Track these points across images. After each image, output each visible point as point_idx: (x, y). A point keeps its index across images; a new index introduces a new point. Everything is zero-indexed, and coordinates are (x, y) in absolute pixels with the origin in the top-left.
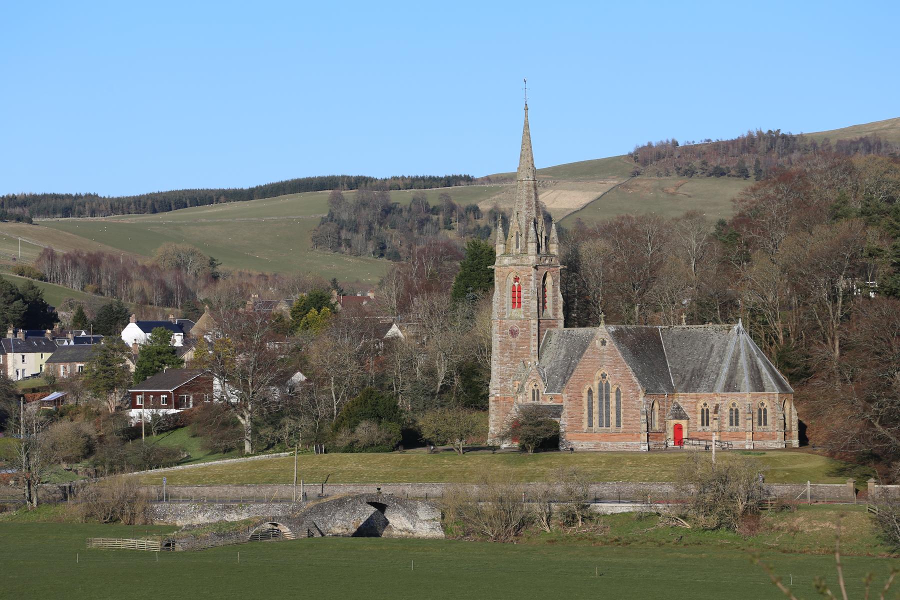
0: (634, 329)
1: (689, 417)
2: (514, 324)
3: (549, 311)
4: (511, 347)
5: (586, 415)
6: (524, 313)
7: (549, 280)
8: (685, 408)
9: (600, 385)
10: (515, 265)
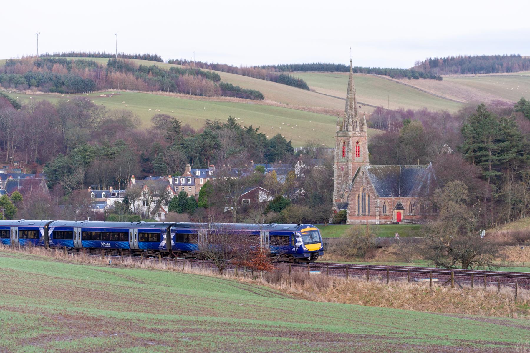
0: (384, 167)
5: (357, 208)
9: (362, 194)
10: (343, 136)
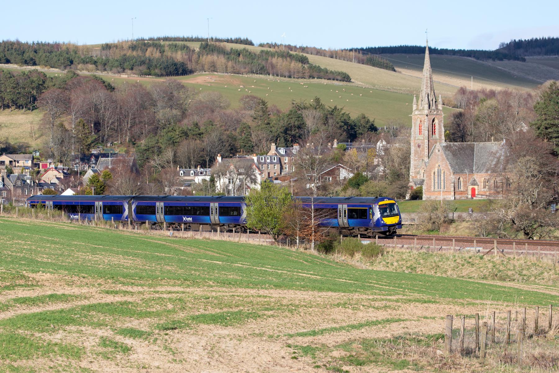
0: (459, 144)
2: (419, 142)
3: (437, 135)
4: (418, 153)
5: (433, 184)
6: (423, 137)
7: (436, 121)
8: (477, 180)
9: (438, 170)
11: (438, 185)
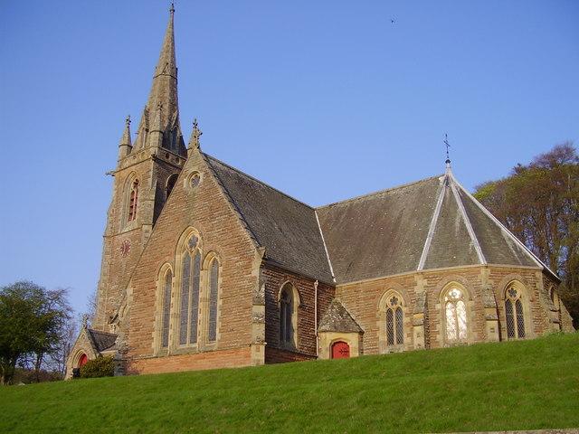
1: (363, 328)
5: (157, 324)
9: (187, 258)
11: (183, 324)
